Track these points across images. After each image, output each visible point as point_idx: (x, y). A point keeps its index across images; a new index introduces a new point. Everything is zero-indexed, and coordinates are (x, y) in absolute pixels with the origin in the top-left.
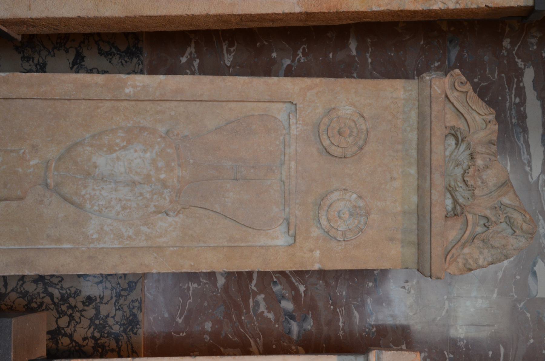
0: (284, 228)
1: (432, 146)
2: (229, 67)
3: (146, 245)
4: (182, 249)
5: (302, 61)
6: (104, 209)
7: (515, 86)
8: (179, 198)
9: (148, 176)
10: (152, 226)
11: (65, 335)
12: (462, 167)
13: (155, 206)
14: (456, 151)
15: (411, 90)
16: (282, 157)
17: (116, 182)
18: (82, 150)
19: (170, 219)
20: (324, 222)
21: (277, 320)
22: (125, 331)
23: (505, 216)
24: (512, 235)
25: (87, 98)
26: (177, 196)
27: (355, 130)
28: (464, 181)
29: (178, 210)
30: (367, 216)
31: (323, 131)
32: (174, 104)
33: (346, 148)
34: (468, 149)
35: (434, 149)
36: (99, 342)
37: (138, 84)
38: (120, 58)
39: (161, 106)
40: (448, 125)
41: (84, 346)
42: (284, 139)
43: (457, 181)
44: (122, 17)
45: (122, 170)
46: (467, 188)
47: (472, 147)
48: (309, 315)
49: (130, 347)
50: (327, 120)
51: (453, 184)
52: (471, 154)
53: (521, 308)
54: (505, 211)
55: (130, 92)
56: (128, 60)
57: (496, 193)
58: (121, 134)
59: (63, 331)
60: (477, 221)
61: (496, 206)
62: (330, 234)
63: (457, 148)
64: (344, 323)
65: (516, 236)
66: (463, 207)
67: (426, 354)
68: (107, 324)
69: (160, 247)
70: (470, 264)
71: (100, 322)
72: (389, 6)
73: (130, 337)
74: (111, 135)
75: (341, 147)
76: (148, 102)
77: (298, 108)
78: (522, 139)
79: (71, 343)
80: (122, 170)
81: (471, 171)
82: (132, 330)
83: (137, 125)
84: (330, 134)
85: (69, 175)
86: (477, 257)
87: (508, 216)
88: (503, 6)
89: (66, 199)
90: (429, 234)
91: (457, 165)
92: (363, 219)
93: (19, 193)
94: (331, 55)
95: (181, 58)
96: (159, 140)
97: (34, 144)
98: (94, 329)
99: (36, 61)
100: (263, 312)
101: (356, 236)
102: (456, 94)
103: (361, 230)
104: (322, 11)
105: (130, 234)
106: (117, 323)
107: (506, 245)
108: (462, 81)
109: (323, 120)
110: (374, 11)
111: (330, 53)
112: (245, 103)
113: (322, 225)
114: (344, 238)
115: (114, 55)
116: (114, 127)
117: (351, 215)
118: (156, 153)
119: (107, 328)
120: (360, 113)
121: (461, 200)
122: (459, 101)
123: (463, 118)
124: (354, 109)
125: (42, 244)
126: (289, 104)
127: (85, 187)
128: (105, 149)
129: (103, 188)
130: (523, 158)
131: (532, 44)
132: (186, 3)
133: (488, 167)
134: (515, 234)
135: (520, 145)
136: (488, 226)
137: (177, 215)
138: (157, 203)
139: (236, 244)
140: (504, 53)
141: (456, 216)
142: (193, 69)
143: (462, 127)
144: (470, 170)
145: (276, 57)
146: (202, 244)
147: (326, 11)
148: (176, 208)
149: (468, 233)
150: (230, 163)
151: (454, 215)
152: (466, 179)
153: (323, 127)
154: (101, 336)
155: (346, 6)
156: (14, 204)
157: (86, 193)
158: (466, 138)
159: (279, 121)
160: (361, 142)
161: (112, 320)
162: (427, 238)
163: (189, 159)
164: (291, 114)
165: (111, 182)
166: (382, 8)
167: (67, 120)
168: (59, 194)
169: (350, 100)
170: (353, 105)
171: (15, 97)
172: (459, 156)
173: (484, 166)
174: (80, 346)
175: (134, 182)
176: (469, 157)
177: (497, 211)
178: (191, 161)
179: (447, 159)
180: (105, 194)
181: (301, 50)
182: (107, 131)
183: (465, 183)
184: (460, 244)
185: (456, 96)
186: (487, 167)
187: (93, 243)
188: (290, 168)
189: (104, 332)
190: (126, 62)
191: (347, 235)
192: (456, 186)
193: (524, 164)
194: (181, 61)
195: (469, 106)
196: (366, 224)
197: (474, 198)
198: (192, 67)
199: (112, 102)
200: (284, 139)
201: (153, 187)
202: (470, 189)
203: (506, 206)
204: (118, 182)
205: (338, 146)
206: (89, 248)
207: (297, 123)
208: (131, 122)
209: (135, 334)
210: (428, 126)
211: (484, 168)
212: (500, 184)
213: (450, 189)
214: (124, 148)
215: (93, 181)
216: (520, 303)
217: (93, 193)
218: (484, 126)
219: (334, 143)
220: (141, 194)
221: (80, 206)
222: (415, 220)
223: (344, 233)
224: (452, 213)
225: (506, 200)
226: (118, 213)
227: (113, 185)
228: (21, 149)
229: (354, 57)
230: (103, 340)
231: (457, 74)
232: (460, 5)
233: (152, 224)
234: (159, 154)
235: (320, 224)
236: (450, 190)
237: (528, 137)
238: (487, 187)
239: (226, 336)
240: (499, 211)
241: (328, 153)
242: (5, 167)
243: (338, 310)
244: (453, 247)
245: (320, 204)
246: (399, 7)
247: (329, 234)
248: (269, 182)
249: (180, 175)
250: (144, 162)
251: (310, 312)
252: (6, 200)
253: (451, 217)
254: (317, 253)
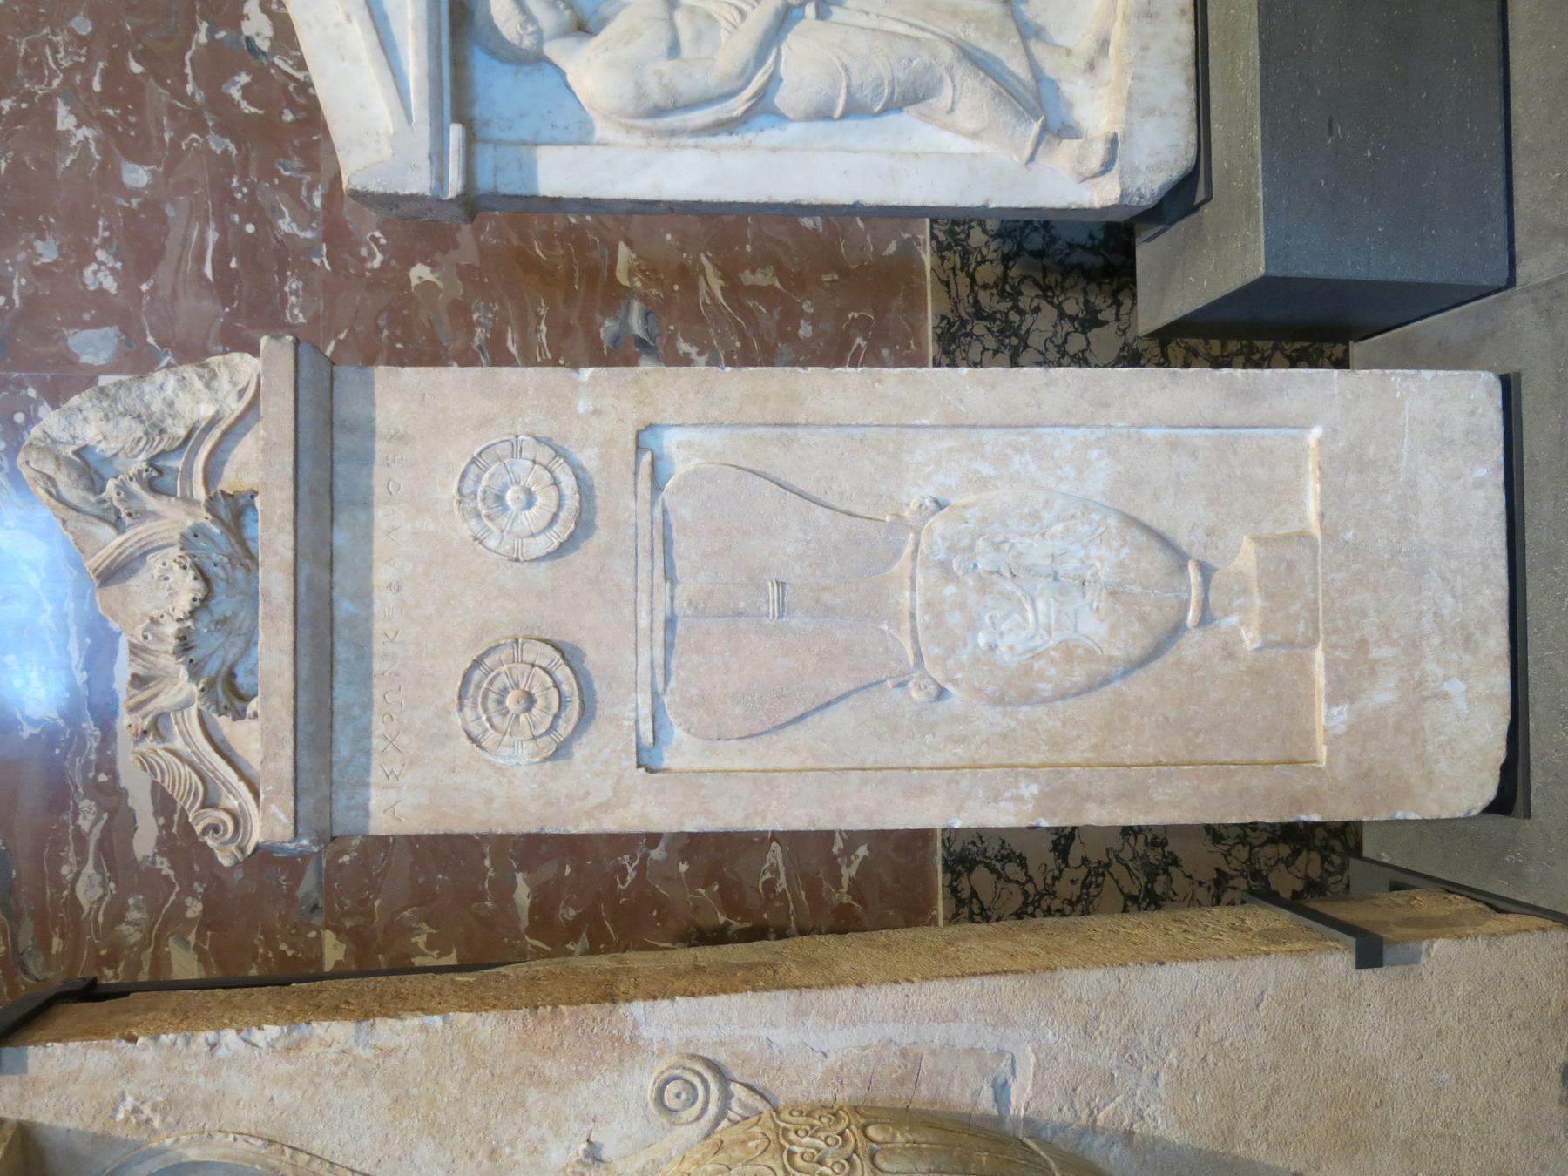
4: (903, 422)
6: (1079, 513)
11: (1072, 319)
14: (230, 658)
15: (351, 808)
18: (1131, 649)
21: (672, 339)
22: (964, 323)
27: (491, 705)
36: (1010, 304)
37: (1010, 806)
38: (985, 850)
39: (955, 754)
41: (1037, 296)
51: (240, 574)
55: (1027, 787)
58: (1046, 689)
63: (228, 664)
64: (538, 331)
67: (369, 265)
70: (201, 377)
74: (1068, 685)
76: (985, 763)
79: (1060, 303)
83: (1009, 709)
96: (959, 676)
100: (699, 354)
102: (233, 803)
105: (1017, 459)
106: (978, 338)
109: (570, 729)
116: (1059, 703)
118: (965, 644)
119: (995, 329)
125: (1207, 437)
127: (1121, 565)
128: (1080, 651)
131: (138, 908)
138: (963, 526)
149: (204, 453)
154: (1006, 314)
157: (1118, 551)
167: (1161, 718)
169: (505, 780)
184: (223, 426)
190: (973, 843)
208: (1021, 716)
209: (943, 317)
220: (997, 547)
222: (340, 485)
223: (516, 450)
226: (1047, 504)
229: (520, 869)
230: (1005, 306)
254: (583, 406)
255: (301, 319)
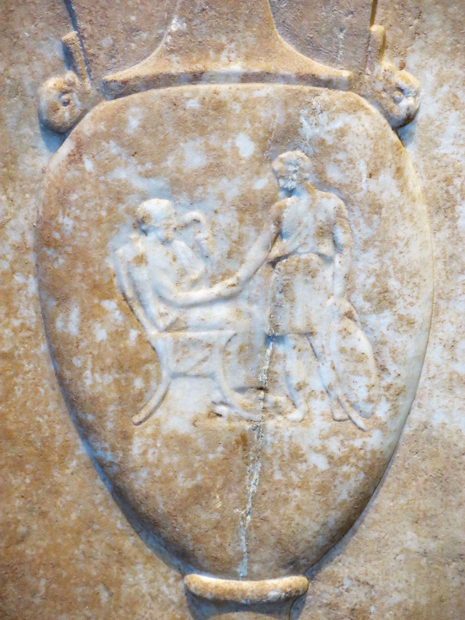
6: (388, 380)
18: (144, 474)
74: (77, 362)
83: (31, 257)
96: (89, 165)
116: (44, 347)
118: (147, 175)
128: (138, 383)
138: (363, 168)
157: (323, 450)
165: (273, 353)
167: (22, 529)
208: (19, 279)
233: (448, 181)
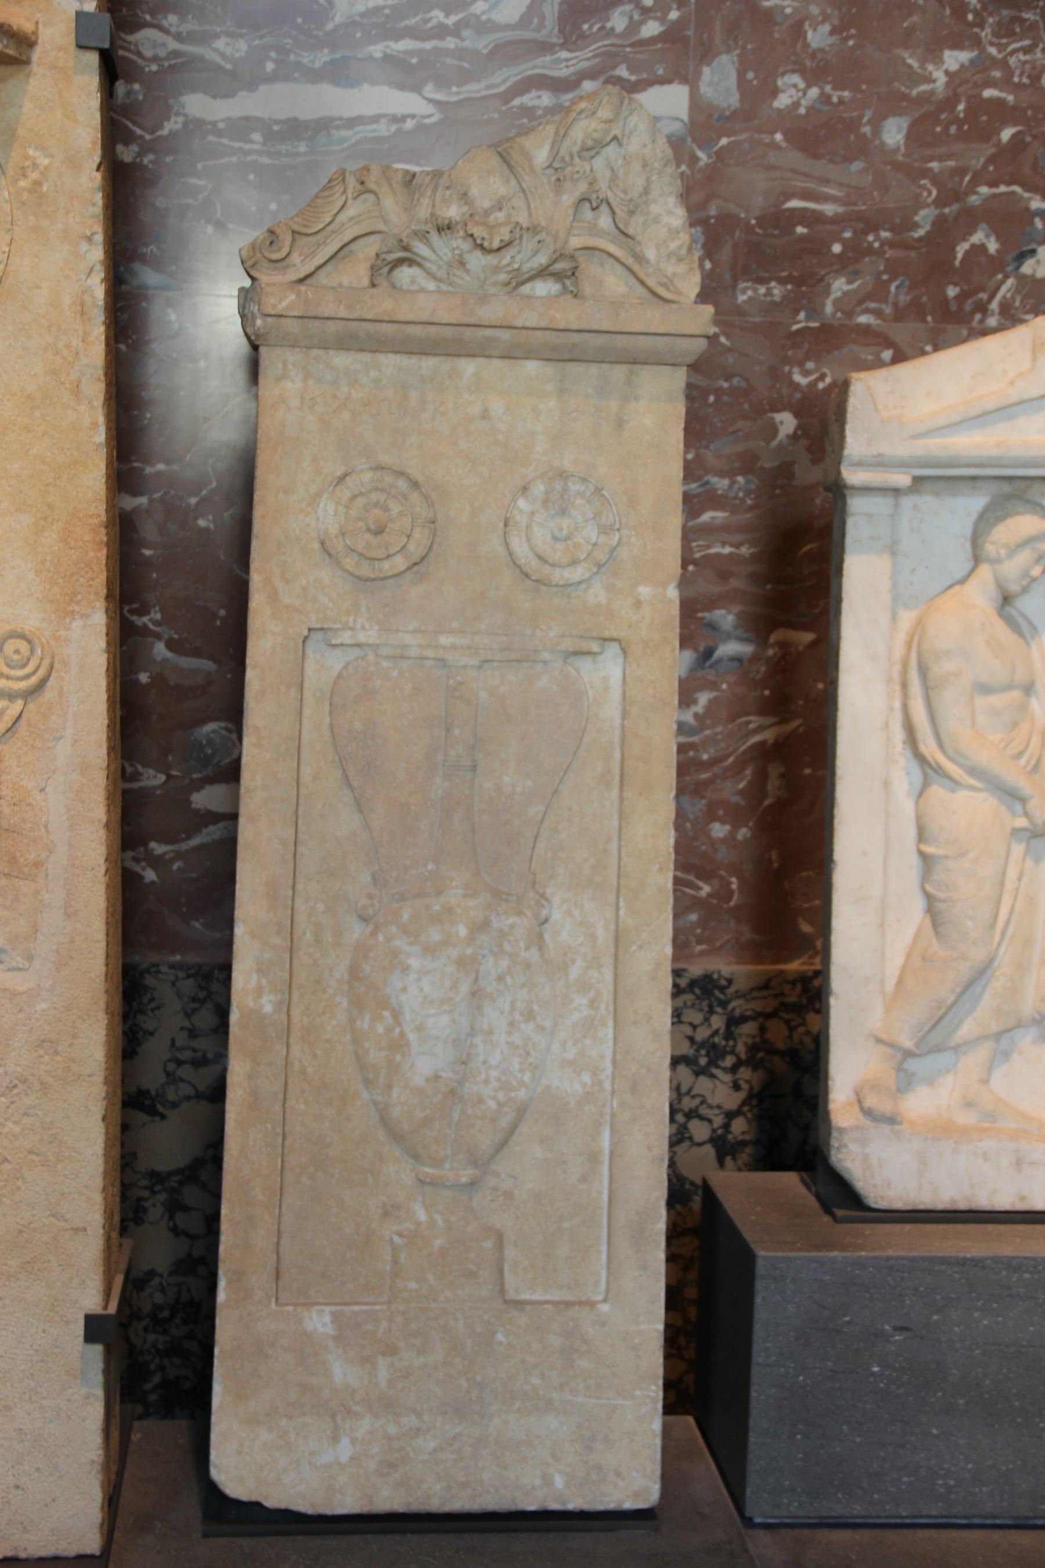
0: (585, 665)
1: (417, 320)
2: (169, 777)
3: (611, 968)
4: (622, 890)
5: (159, 616)
6: (531, 1060)
7: (225, 141)
8: (512, 895)
9: (461, 962)
10: (569, 955)
11: (726, 1127)
12: (468, 252)
13: (527, 948)
14: (427, 265)
15: (285, 364)
16: (428, 663)
17: (472, 1033)
19: (556, 915)
20: (576, 574)
21: (713, 686)
22: (724, 1004)
23: (577, 160)
24: (620, 145)
25: (281, 1096)
26: (506, 900)
27: (374, 497)
28: (499, 249)
29: (537, 897)
30: (567, 478)
31: (374, 569)
32: (300, 905)
33: (412, 518)
34: (427, 235)
35: (425, 316)
36: (743, 1056)
37: (253, 984)
38: (143, 1013)
39: (304, 933)
40: (366, 282)
41: (751, 1088)
42: (388, 658)
43: (497, 267)
44: (106, 1021)
45: (445, 1019)
46: (516, 243)
47: (423, 227)
48: (703, 618)
49: (755, 994)
50: (348, 560)
51: (503, 277)
52: (439, 230)
53: (709, 157)
54: (567, 159)
55: (270, 1001)
56: (149, 996)
57: (526, 178)
58: (364, 1023)
59: (720, 1132)
60: (586, 225)
61: (553, 178)
62: (604, 561)
63: (423, 262)
64: (724, 544)
65: (623, 136)
66: (558, 254)
67: (796, 370)
68: (708, 1039)
69: (617, 938)
70: (680, 247)
71: (703, 1056)
72: (95, 403)
73: (737, 992)
74: (367, 1045)
75: (412, 530)
76: (295, 961)
77: (319, 626)
78: (344, 133)
79: (744, 1114)
80: (445, 1019)
81: (478, 231)
82: (722, 989)
83: (346, 987)
84: (381, 553)
85: (453, 1136)
86: (665, 230)
87: (579, 152)
88: (99, 127)
89: (505, 1143)
90: (613, 336)
91: (462, 264)
92: (574, 487)
93: (488, 1244)
94: (147, 552)
95: (147, 880)
96: (381, 938)
97: (380, 1211)
98: (718, 1067)
99: (145, 1193)
100: (696, 715)
101: (610, 504)
102: (295, 258)
103: (598, 490)
104: (104, 562)
105: (584, 1001)
106: (707, 1020)
107: (644, 160)
108: (268, 243)
109: (348, 568)
110: (107, 439)
111: (143, 555)
112: (303, 742)
113: (583, 578)
114: (612, 529)
115: (136, 1025)
116: (348, 1037)
117: (563, 512)
118: (411, 944)
119: (716, 1040)
120: (335, 483)
121: (542, 259)
122: (313, 252)
123: (353, 246)
124: (325, 496)
125: (600, 1193)
126: (307, 643)
127: (480, 1100)
128: (398, 1057)
129: (484, 1062)
130: (386, 134)
131: (128, 94)
132: (78, 875)
133: (465, 194)
134: (619, 136)
135: (357, 137)
136: (599, 201)
137: (547, 900)
138: (522, 944)
139: (617, 771)
140: (150, 162)
141: (576, 274)
142: (171, 855)
143: (372, 252)
144: (476, 235)
145: (148, 674)
146: (614, 846)
147: (105, 551)
148: (532, 903)
149: (612, 249)
150: (438, 780)
151: (573, 278)
152: (496, 244)
153: (365, 570)
154: (732, 1052)
155: (94, 504)
156: (511, 1253)
157: (494, 1098)
158: (401, 241)
159: (345, 667)
160: (402, 484)
161: (699, 1030)
162: (622, 341)
163: (427, 871)
164: (330, 641)
165: (471, 1043)
166: (101, 419)
167: (328, 1140)
168: (492, 1157)
169: (304, 506)
170: (314, 500)
171: (275, 1257)
172: (441, 258)
173: (462, 202)
174: (750, 1096)
175: (473, 994)
176: (446, 235)
177: (565, 177)
178: (430, 866)
179: (444, 287)
180: (495, 1059)
181: (134, 618)
182: (356, 1054)
183: (504, 247)
184: (636, 268)
185: (302, 258)
186: (464, 197)
187: (601, 1084)
188: (454, 647)
189: (725, 1047)
190: (152, 1000)
191: (609, 523)
192: (509, 268)
193: (399, 132)
194: (153, 882)
195: (323, 229)
196: (584, 480)
197: (540, 228)
198: (167, 857)
199: (291, 1040)
200: (388, 658)
201: (485, 952)
202: (518, 236)
203: (555, 154)
204: (472, 1028)
205: (408, 536)
206: (613, 1093)
207: (352, 629)
208: (338, 999)
209: (730, 981)
210: (370, 327)
211: (466, 203)
212: (505, 167)
213: (514, 284)
214: (396, 1015)
215: (467, 1085)
216: (698, 159)
217: (494, 1084)
218: (371, 197)
219: (403, 544)
220: (500, 978)
221: (521, 1112)
222: (577, 369)
223: (605, 530)
224: (568, 282)
225: (541, 156)
226: (541, 1029)
227: (478, 1040)
228: (392, 1242)
229: (151, 500)
230: (741, 1049)
231: (251, 254)
232: (95, 233)
233: (565, 954)
234: (412, 939)
235: (580, 583)
236: (517, 281)
237: (340, 118)
238: (510, 199)
239: (742, 793)
240: (566, 172)
241: (423, 559)
242: (430, 1277)
243: (697, 555)
244: (642, 283)
245: (537, 581)
246: (99, 379)
247: (604, 564)
248: (483, 695)
249: (460, 891)
250: (428, 972)
251: (700, 615)
252: (501, 1271)
253: (576, 284)
254: (645, 591)
255: (742, 298)
